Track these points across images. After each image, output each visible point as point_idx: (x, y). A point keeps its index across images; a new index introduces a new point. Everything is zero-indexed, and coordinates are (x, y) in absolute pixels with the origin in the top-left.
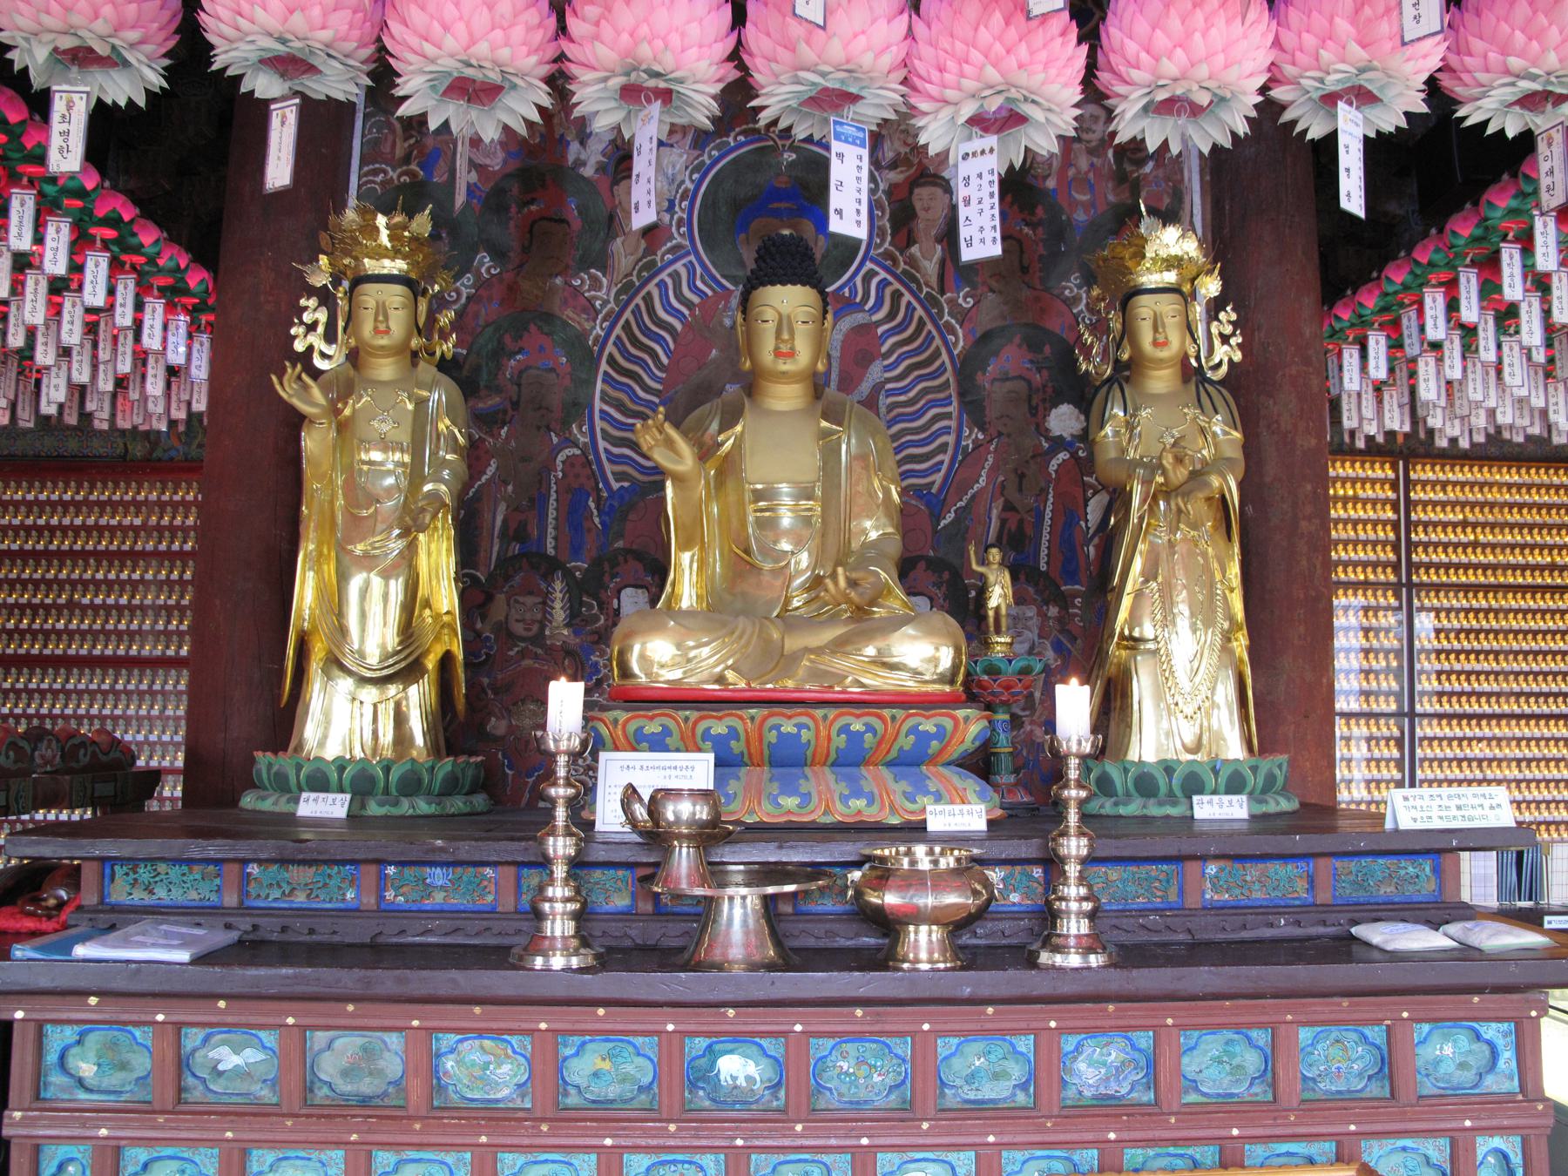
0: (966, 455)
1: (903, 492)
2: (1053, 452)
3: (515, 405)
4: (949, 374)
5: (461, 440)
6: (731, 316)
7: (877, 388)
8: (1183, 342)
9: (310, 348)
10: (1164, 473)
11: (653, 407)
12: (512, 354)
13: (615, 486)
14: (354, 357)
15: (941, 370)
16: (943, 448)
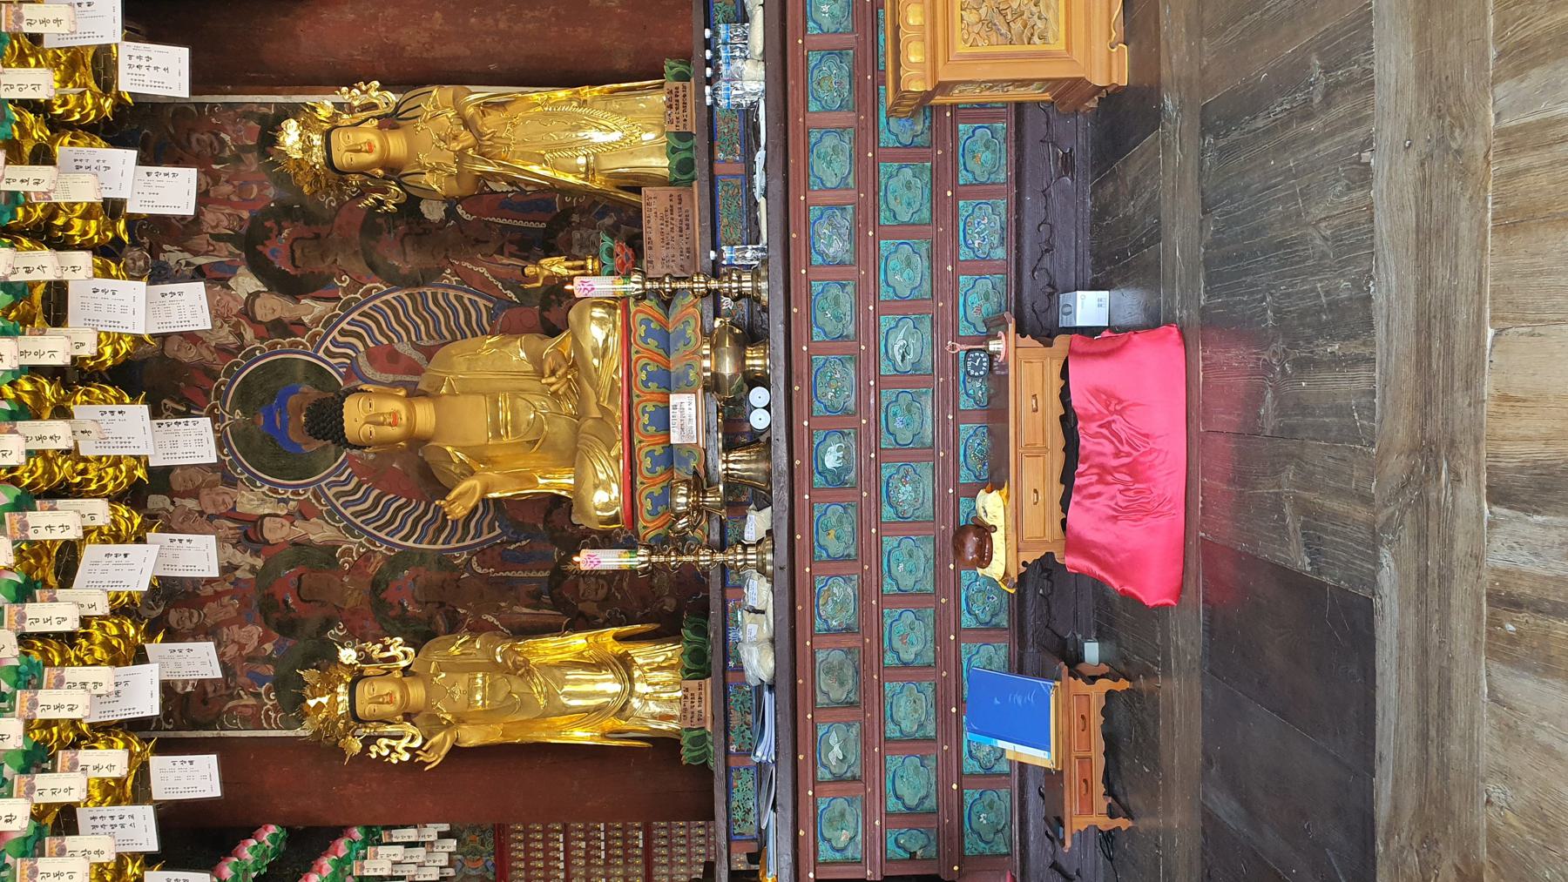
0: (463, 282)
1: (493, 334)
2: (458, 217)
4: (403, 294)
5: (466, 638)
6: (370, 455)
7: (415, 346)
8: (366, 130)
9: (406, 749)
12: (404, 609)
13: (498, 531)
14: (408, 717)
16: (459, 299)
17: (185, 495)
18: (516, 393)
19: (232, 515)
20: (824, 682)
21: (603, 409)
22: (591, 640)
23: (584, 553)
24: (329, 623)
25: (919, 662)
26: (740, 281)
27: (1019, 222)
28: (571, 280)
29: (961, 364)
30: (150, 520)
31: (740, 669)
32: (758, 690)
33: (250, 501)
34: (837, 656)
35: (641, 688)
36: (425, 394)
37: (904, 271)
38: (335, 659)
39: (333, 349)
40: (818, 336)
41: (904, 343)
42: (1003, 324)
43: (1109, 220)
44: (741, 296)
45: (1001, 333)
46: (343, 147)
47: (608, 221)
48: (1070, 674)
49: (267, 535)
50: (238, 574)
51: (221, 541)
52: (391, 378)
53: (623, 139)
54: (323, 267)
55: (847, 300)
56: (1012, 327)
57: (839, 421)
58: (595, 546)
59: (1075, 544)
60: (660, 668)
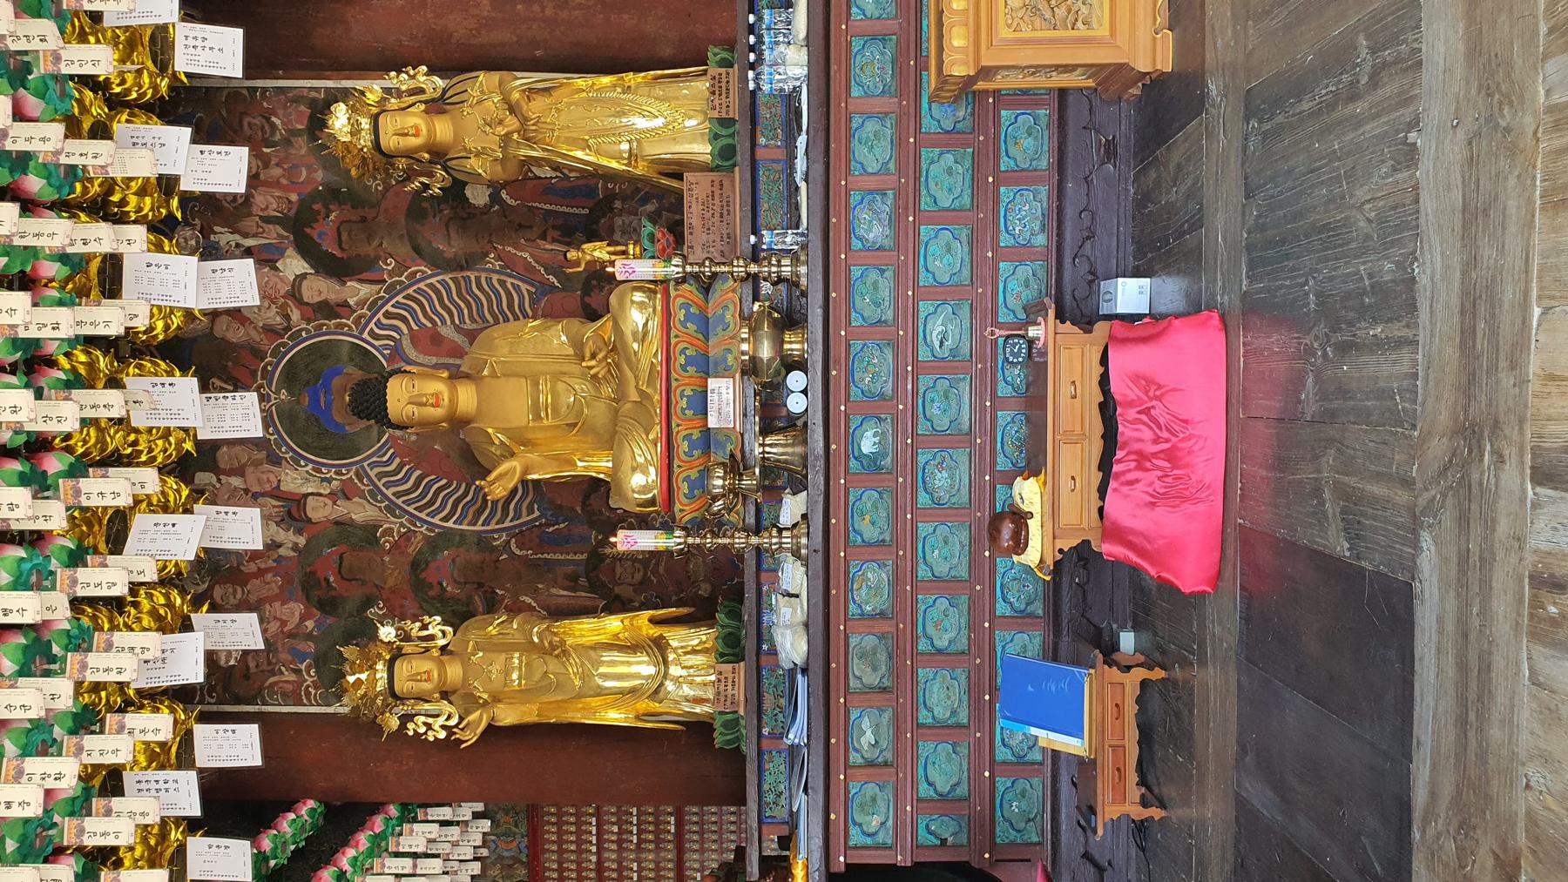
1: (535, 318)
2: (502, 202)
3: (480, 585)
4: (447, 278)
6: (411, 436)
7: (458, 329)
8: (414, 114)
9: (443, 727)
10: (512, 133)
11: (480, 488)
12: (443, 589)
13: (537, 513)
14: (445, 695)
15: (443, 283)
16: (502, 283)
17: (230, 473)
18: (557, 376)
19: (276, 493)
20: (857, 667)
21: (641, 393)
22: (627, 622)
23: (621, 533)
24: (369, 602)
25: (953, 649)
26: (779, 266)
27: (1060, 210)
28: (612, 263)
29: (1000, 351)
30: (198, 494)
31: (774, 652)
32: (792, 673)
33: (294, 480)
34: (870, 641)
35: (675, 671)
36: (467, 376)
37: (945, 256)
38: (374, 637)
39: (377, 331)
40: (856, 321)
41: (943, 329)
42: (1043, 310)
43: (1151, 207)
44: (780, 280)
45: (1040, 319)
46: (391, 130)
47: (650, 207)
48: (1105, 662)
49: (310, 513)
50: (282, 551)
51: (266, 518)
52: (434, 360)
53: (666, 126)
54: (367, 250)
55: (885, 290)
56: (1051, 313)
57: (875, 407)
58: (631, 527)
59: (1113, 532)
60: (694, 652)
